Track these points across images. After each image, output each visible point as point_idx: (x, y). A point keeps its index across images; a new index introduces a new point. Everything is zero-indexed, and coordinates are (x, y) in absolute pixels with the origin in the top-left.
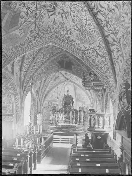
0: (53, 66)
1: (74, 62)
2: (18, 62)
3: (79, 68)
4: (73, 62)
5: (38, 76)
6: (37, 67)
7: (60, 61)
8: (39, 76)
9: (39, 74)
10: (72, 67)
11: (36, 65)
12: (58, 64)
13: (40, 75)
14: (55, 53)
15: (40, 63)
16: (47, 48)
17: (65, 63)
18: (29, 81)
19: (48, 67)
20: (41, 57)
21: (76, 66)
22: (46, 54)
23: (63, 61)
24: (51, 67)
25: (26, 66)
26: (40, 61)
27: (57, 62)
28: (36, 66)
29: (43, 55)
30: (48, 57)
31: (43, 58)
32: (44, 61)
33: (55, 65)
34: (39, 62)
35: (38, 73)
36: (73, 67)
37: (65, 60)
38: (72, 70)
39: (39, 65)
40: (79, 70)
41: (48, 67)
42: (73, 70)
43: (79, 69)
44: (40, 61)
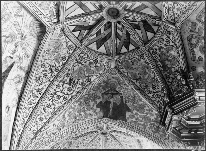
0: (88, 112)
1: (131, 104)
2: (16, 80)
3: (140, 116)
4: (128, 104)
5: (54, 132)
6: (54, 108)
7: (101, 102)
8: (56, 133)
9: (57, 128)
10: (125, 115)
11: (53, 104)
12: (98, 110)
13: (58, 130)
15: (62, 99)
16: (80, 65)
17: (111, 106)
18: (32, 139)
19: (77, 113)
20: (65, 85)
22: (76, 80)
23: (108, 103)
24: (83, 114)
25: (32, 98)
26: (61, 94)
27: (95, 106)
28: (53, 107)
29: (71, 80)
30: (80, 86)
31: (69, 89)
32: (70, 96)
33: (91, 112)
34: (59, 97)
35: (54, 125)
36: (128, 114)
37: (112, 100)
38: (126, 121)
39: (60, 105)
40: (141, 121)
41: (77, 113)
42: (128, 121)
43: (141, 119)
44: (61, 94)
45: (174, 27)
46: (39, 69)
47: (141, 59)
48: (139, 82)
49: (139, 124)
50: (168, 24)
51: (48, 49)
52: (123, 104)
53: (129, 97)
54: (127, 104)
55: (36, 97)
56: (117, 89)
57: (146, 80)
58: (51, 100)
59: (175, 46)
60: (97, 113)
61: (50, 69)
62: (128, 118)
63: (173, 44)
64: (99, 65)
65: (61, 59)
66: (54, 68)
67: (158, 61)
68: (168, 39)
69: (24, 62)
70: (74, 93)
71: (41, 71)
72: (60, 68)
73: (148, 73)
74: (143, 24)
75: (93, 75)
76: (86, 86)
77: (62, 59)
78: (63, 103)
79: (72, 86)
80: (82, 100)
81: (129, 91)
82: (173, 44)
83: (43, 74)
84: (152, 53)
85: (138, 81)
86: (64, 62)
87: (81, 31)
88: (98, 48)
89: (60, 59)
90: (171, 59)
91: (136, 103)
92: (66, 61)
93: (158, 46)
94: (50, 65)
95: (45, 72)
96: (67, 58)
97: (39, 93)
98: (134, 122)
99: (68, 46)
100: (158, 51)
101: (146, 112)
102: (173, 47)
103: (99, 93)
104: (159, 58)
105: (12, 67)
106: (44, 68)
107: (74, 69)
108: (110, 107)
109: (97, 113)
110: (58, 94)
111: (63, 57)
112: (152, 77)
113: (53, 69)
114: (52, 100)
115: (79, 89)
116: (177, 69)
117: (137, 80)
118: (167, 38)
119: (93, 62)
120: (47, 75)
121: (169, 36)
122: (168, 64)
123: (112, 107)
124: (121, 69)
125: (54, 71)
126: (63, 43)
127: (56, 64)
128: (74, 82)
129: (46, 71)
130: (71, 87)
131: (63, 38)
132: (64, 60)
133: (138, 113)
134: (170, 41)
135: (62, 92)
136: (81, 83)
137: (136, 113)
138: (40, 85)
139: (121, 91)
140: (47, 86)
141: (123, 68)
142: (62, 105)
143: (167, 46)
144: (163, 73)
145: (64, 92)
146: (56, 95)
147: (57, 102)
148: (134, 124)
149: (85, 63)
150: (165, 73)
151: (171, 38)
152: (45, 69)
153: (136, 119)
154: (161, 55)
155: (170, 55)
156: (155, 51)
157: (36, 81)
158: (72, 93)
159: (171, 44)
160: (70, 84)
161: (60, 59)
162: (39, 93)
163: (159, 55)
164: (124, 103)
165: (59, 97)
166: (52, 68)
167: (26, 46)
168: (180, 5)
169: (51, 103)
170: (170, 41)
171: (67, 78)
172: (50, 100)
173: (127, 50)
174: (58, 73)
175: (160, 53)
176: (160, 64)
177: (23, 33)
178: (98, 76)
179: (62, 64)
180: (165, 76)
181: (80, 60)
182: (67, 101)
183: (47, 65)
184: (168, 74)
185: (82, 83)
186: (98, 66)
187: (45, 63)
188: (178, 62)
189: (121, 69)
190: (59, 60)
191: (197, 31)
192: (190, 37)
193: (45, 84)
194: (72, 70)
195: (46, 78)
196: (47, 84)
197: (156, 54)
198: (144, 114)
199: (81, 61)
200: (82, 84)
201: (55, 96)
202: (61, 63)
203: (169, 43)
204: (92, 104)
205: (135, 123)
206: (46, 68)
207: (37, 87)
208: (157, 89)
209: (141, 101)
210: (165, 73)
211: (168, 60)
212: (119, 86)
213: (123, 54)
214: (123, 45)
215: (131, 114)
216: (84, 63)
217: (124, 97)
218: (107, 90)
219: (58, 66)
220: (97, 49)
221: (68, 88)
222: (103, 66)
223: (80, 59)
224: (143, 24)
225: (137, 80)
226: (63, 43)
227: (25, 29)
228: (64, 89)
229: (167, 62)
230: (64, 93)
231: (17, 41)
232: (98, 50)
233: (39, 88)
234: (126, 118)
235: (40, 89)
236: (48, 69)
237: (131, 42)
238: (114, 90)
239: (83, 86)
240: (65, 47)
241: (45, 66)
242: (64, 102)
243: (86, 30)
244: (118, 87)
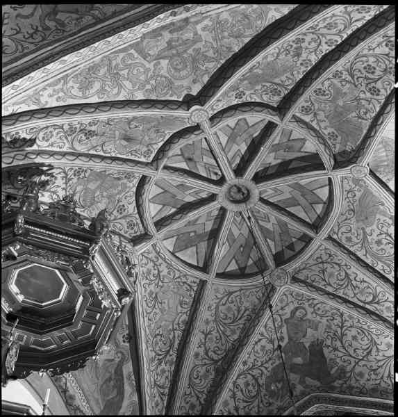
16: (277, 81)
29: (298, 55)
47: (146, 149)
51: (360, 120)
53: (127, 71)
57: (114, 131)
58: (353, 20)
61: (356, 77)
65: (327, 92)
66: (344, 78)
77: (325, 92)
81: (138, 85)
83: (376, 74)
87: (289, 140)
89: (329, 91)
91: (105, 75)
93: (129, 187)
94: (354, 84)
95: (370, 76)
100: (125, 181)
106: (373, 84)
107: (292, 74)
114: (351, 20)
119: (245, 91)
125: (344, 73)
127: (339, 85)
129: (366, 78)
138: (387, 55)
152: (370, 83)
161: (329, 91)
163: (119, 179)
166: (349, 78)
168: (152, 281)
175: (120, 182)
184: (83, 175)
187: (368, 95)
190: (332, 91)
194: (295, 72)
208: (81, 137)
216: (268, 84)
217: (141, 60)
218: (190, 51)
235: (387, 45)
236: (361, 80)
237: (180, 157)
238: (171, 58)
241: (370, 89)
243: (278, 144)
244: (165, 69)
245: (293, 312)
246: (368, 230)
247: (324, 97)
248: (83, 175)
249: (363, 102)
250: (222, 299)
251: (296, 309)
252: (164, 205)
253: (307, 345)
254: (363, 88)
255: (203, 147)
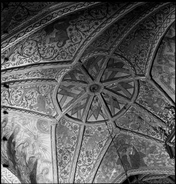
4: (141, 151)
6: (84, 181)
12: (120, 166)
14: (105, 142)
15: (86, 170)
16: (89, 137)
17: (128, 157)
20: (84, 159)
21: (149, 155)
22: (91, 151)
26: (85, 167)
29: (87, 152)
30: (96, 154)
32: (92, 165)
34: (84, 170)
36: (145, 159)
37: (127, 154)
38: (146, 165)
39: (87, 176)
40: (158, 161)
43: (157, 159)
44: (85, 167)
45: (145, 78)
46: (58, 155)
47: (133, 111)
48: (141, 130)
49: (158, 164)
50: (139, 77)
52: (138, 152)
53: (140, 145)
54: (140, 151)
55: (66, 179)
56: (127, 143)
57: (145, 125)
58: (79, 176)
59: (154, 90)
60: (119, 170)
61: (67, 152)
62: (147, 163)
63: (151, 89)
64: (103, 131)
65: (72, 140)
67: (147, 107)
68: (146, 87)
69: (45, 156)
70: (94, 162)
71: (61, 156)
72: (75, 147)
73: (145, 119)
74: (121, 85)
75: (102, 140)
76: (101, 152)
77: (73, 139)
78: (89, 173)
79: (90, 157)
80: (103, 165)
82: (151, 89)
84: (140, 103)
85: (140, 129)
86: (75, 141)
87: (77, 112)
88: (96, 118)
90: (156, 101)
91: (147, 147)
92: (76, 139)
94: (66, 148)
95: (64, 156)
96: (76, 137)
97: (66, 174)
98: (152, 164)
99: (73, 127)
100: (143, 100)
101: (159, 151)
102: (153, 91)
103: (114, 152)
104: (147, 104)
105: (37, 164)
106: (62, 153)
108: (128, 160)
109: (119, 170)
110: (82, 168)
111: (73, 138)
112: (149, 121)
113: (70, 150)
115: (97, 157)
116: (165, 106)
117: (138, 129)
118: (145, 87)
120: (67, 157)
121: (145, 84)
122: (157, 105)
123: (130, 159)
124: (122, 126)
125: (71, 151)
126: (68, 127)
128: (90, 152)
130: (90, 157)
131: (67, 124)
132: (75, 140)
133: (153, 155)
134: (148, 88)
135: (84, 165)
136: (96, 151)
137: (151, 155)
138: (64, 168)
139: (130, 143)
140: (71, 166)
141: (123, 125)
142: (88, 175)
143: (148, 93)
144: (156, 115)
145: (86, 164)
146: (81, 170)
147: (84, 175)
148: (153, 165)
149: (92, 134)
150: (157, 114)
151: (147, 85)
153: (154, 161)
154: (147, 101)
155: (154, 99)
156: (141, 100)
157: (60, 166)
158: (93, 163)
159: (150, 90)
160: (88, 156)
162: (67, 174)
163: (146, 102)
164: (138, 151)
165: (84, 170)
167: (41, 143)
168: (140, 60)
169: (80, 178)
170: (148, 88)
171: (83, 152)
172: (78, 175)
173: (119, 109)
174: (75, 151)
175: (145, 100)
176: (150, 108)
177: (34, 134)
178: (106, 140)
179: (75, 142)
180: (159, 116)
181: (87, 134)
182: (91, 170)
183: (63, 149)
184: (161, 113)
185: (97, 150)
186: (103, 132)
187: (61, 148)
188: (163, 101)
189: (122, 126)
191: (165, 71)
192: (161, 78)
193: (68, 165)
195: (67, 159)
196: (69, 164)
197: (143, 102)
198: (158, 154)
199: (88, 134)
200: (98, 152)
201: (80, 171)
202: (73, 142)
203: (148, 89)
204: (112, 164)
205: (154, 165)
206: (64, 152)
207: (63, 170)
209: (150, 144)
210: (157, 114)
211: (154, 103)
212: (127, 140)
213: (117, 114)
214: (114, 107)
215: (148, 158)
216: (91, 135)
217: (135, 147)
218: (119, 147)
219: (72, 146)
220: (96, 119)
221: (88, 160)
222: (107, 130)
223: (86, 133)
224: (121, 85)
225: (138, 129)
226: (68, 127)
227: (34, 131)
228: (85, 162)
229: (154, 105)
230: (87, 165)
231: (32, 143)
232: (97, 120)
233: (65, 171)
234: (145, 163)
235: (66, 171)
236: (66, 152)
238: (124, 144)
239: (98, 153)
240: (70, 129)
241: (62, 151)
242: (90, 172)
243: (81, 109)
245: (64, 43)
246: (38, 94)
247: (73, 136)
248: (161, 113)
249: (61, 144)
250: (104, 44)
251: (63, 45)
252: (127, 83)
253: (55, 29)
254: (63, 149)
255: (110, 106)
